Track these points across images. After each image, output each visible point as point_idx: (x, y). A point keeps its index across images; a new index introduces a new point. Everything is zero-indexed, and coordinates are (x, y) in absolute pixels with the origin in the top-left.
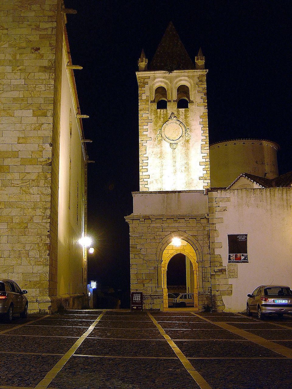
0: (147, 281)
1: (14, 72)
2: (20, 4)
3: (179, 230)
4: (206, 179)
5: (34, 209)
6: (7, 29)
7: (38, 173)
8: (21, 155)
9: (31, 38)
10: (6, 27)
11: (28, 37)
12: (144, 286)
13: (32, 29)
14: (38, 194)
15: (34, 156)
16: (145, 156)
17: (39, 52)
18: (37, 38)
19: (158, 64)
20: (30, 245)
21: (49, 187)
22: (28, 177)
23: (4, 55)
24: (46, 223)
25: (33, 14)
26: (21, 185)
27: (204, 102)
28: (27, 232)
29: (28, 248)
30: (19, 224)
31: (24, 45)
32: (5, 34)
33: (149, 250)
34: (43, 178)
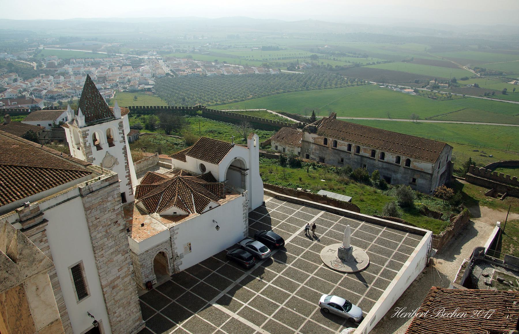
6: (99, 218)
9: (112, 217)
10: (98, 218)
13: (111, 212)
18: (115, 216)
19: (90, 115)
25: (109, 204)
29: (132, 310)
30: (127, 303)
31: (109, 223)
33: (148, 264)
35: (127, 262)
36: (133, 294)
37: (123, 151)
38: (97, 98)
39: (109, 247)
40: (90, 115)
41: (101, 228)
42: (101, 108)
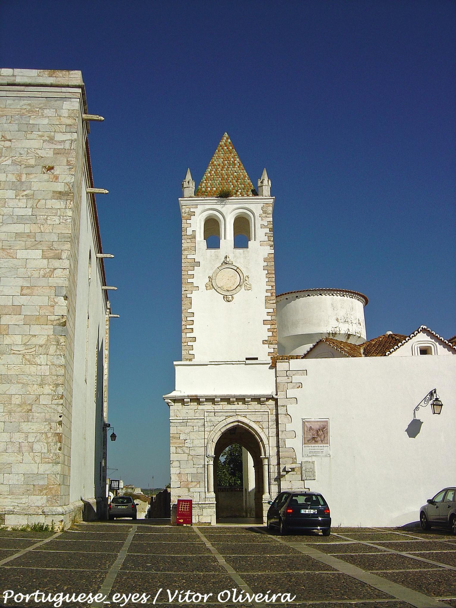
0: (194, 484)
1: (18, 198)
2: (29, 108)
3: (237, 415)
4: (272, 344)
5: (41, 385)
6: (10, 140)
7: (48, 336)
8: (26, 311)
9: (41, 153)
10: (8, 138)
11: (39, 152)
12: (189, 490)
13: (44, 141)
14: (47, 365)
15: (42, 312)
16: (189, 311)
17: (53, 172)
18: (51, 154)
20: (35, 435)
21: (62, 356)
22: (34, 341)
23: (5, 174)
24: (58, 404)
25: (46, 121)
26: (24, 352)
27: (269, 241)
28: (31, 417)
30: (20, 405)
31: (32, 162)
32: (7, 147)
34: (53, 343)
35: (52, 281)
36: (48, 389)
37: (266, 264)
38: (231, 167)
39: (16, 217)
40: (209, 189)
41: (9, 162)
42: (234, 181)
